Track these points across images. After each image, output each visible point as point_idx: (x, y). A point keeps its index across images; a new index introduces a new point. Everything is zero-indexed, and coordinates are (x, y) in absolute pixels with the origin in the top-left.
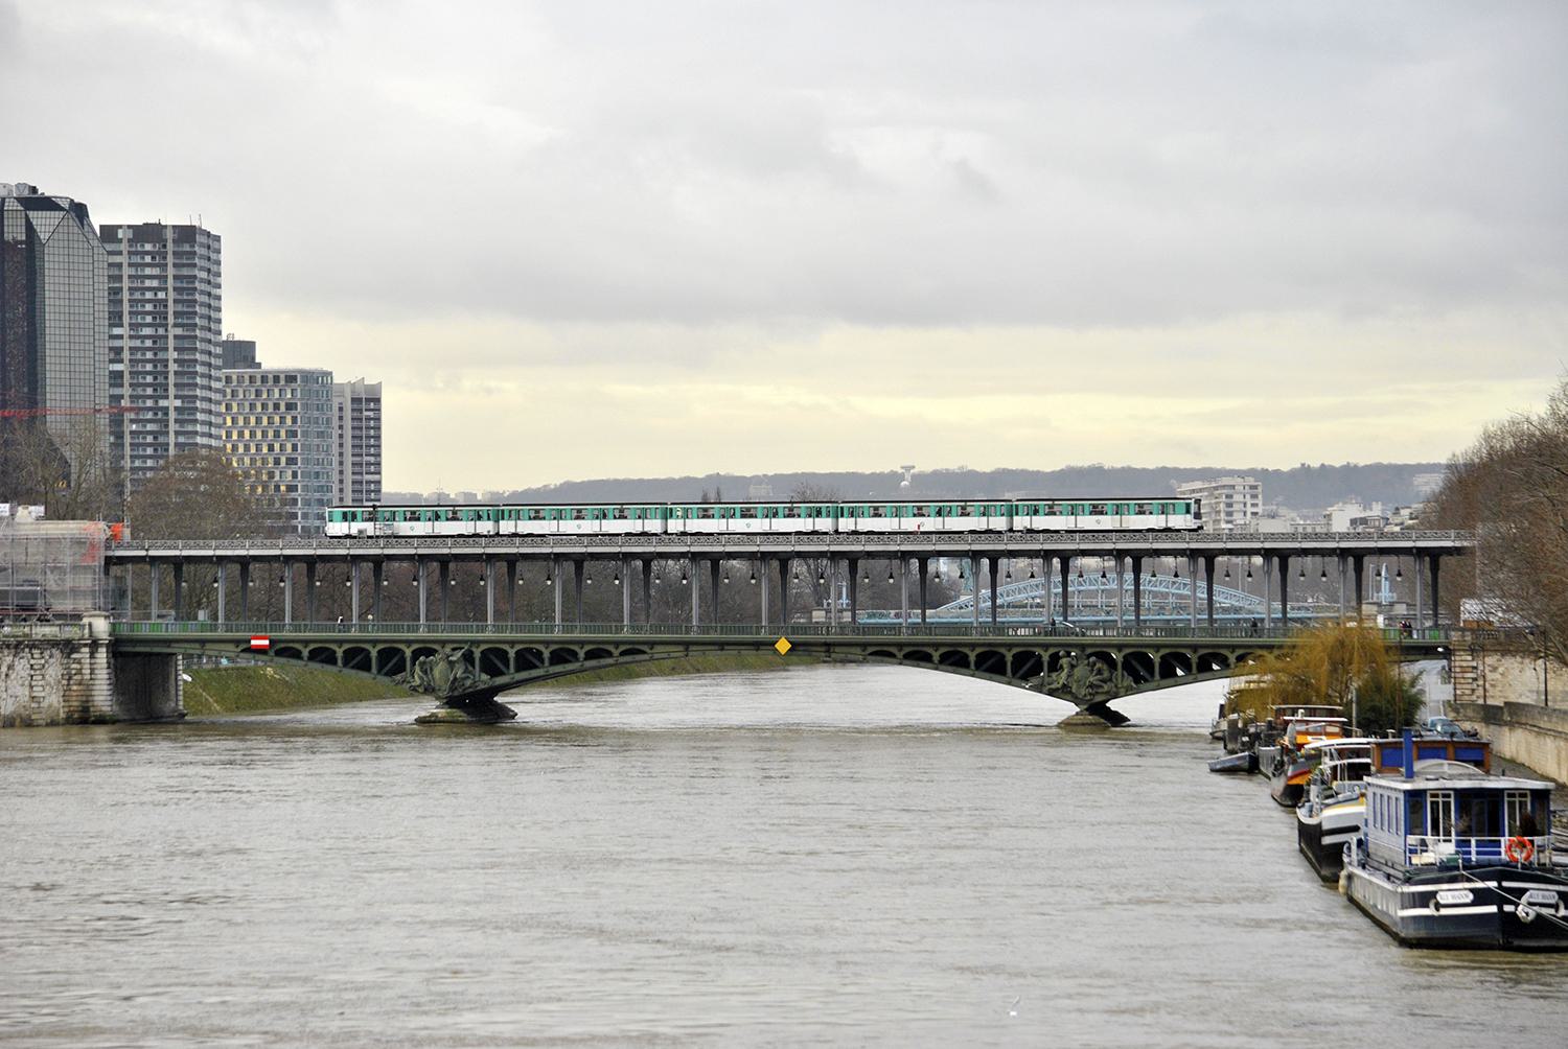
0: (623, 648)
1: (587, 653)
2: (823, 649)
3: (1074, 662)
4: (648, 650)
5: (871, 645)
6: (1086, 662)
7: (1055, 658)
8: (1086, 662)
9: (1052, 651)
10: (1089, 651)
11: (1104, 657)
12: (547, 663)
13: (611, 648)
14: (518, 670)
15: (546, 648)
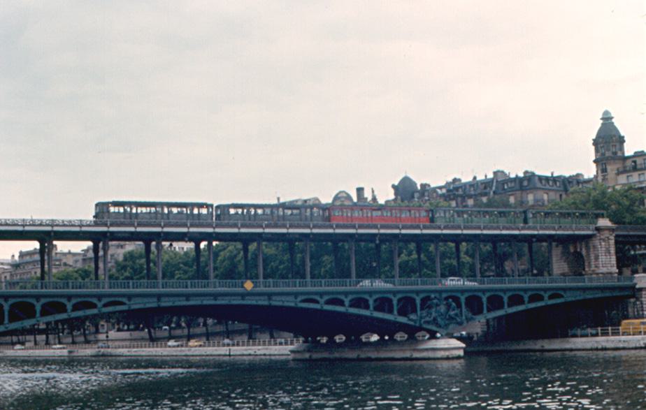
0: (105, 301)
1: (43, 306)
2: (266, 297)
3: (439, 303)
4: (127, 302)
5: (302, 294)
6: (445, 302)
7: (424, 301)
8: (445, 302)
9: (422, 296)
10: (444, 295)
11: (456, 300)
12: (38, 314)
13: (95, 301)
14: (11, 321)
15: (38, 302)
